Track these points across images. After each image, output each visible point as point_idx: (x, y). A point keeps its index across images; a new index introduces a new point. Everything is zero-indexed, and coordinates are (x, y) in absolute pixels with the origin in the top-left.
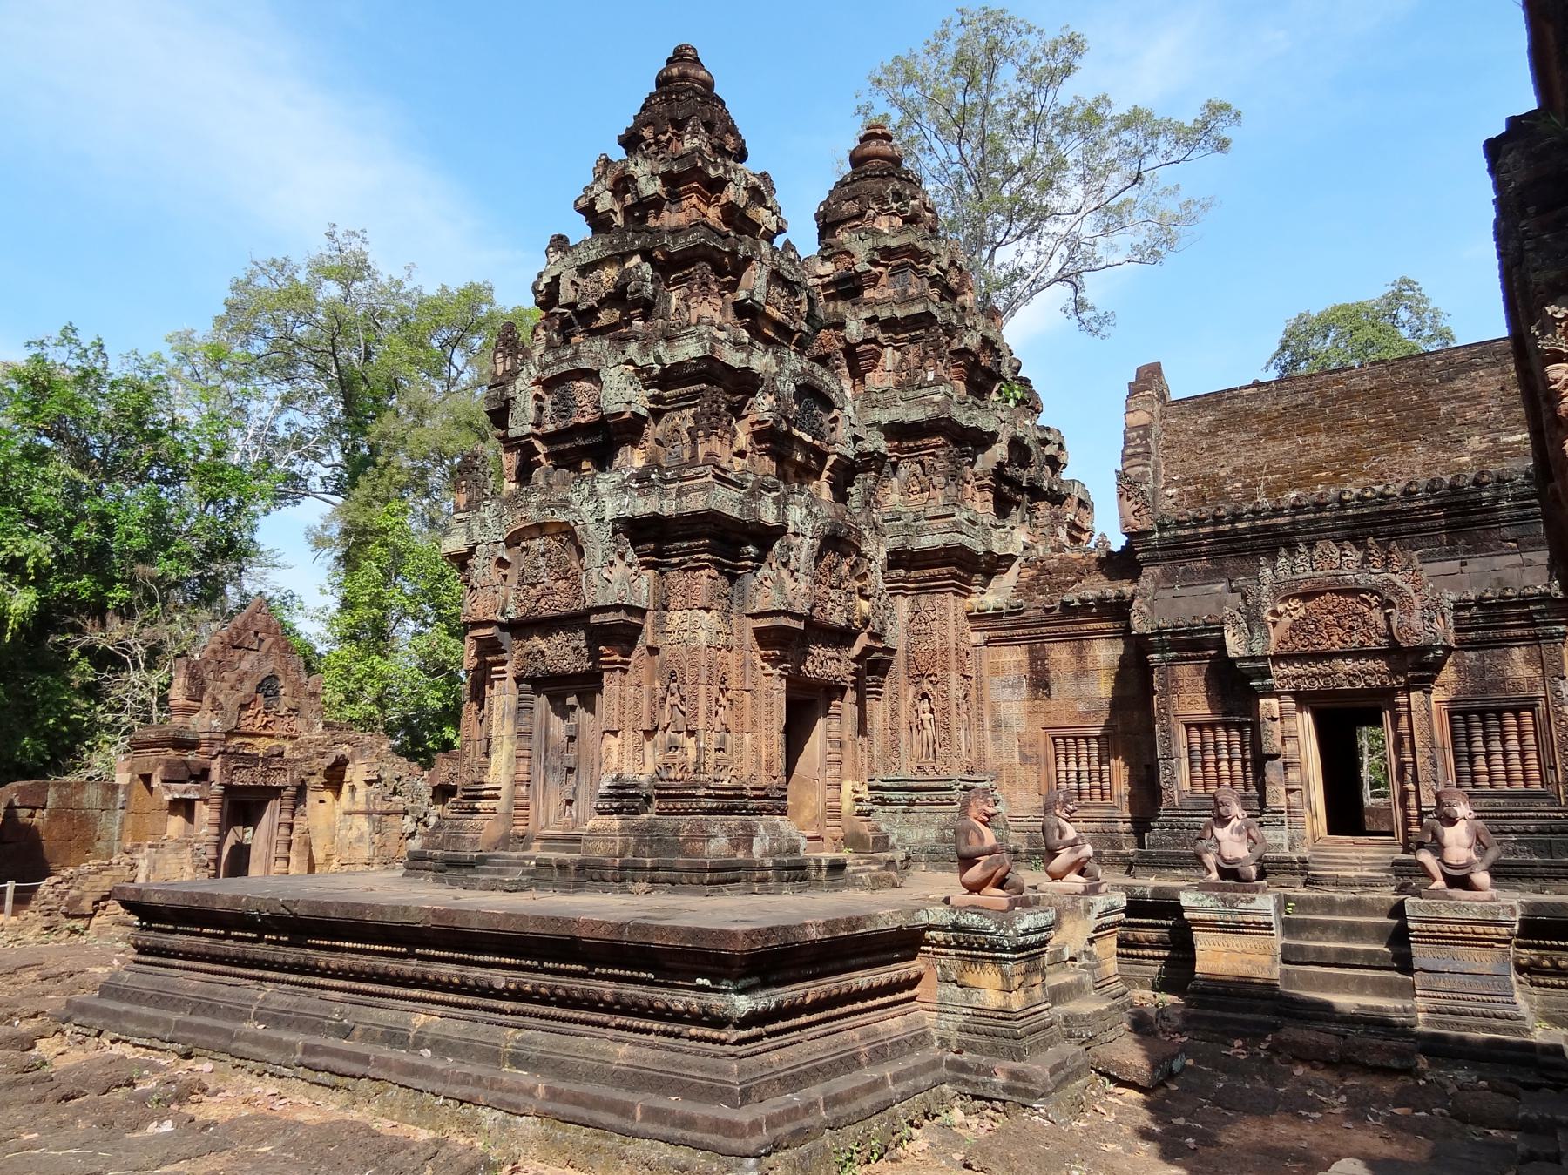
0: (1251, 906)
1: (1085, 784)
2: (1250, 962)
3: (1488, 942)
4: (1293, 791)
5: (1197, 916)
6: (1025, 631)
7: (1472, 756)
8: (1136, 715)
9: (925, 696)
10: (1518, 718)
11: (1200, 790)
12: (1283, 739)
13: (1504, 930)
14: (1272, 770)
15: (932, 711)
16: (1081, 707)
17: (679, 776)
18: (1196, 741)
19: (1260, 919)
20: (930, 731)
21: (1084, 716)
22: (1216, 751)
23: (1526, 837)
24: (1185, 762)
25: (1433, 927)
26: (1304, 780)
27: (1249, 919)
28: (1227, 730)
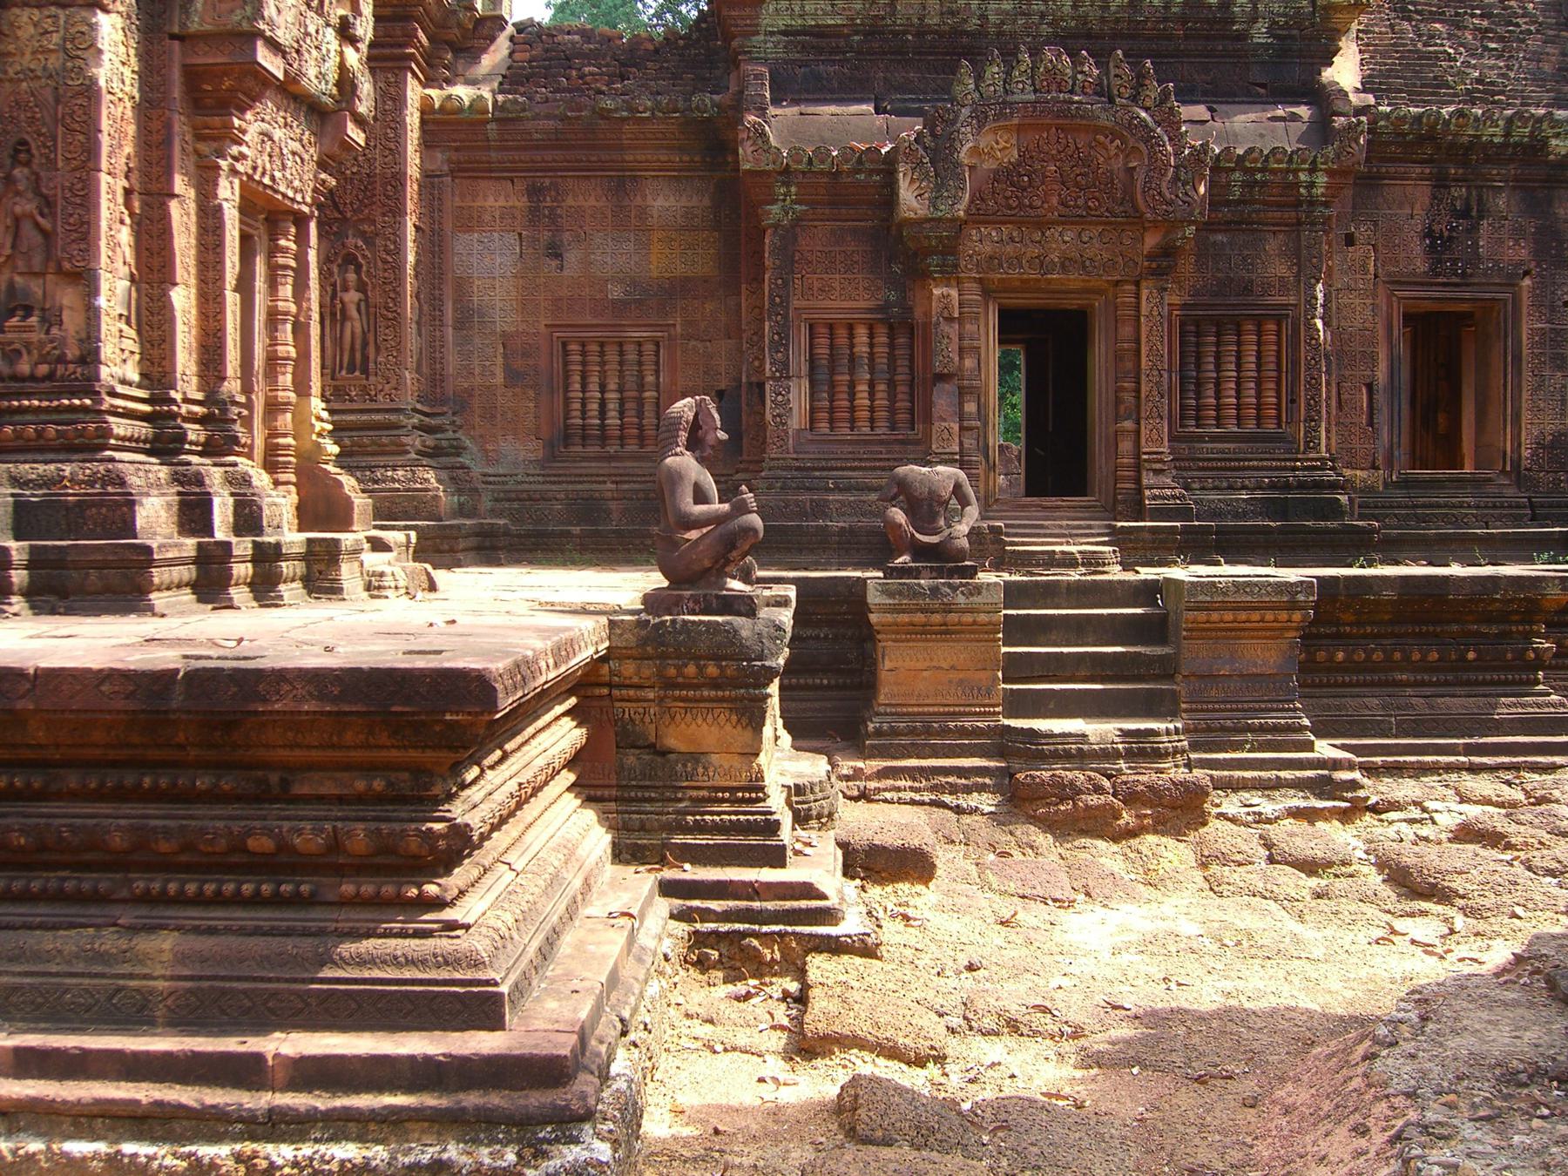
0: (975, 599)
1: (613, 420)
2: (961, 681)
3: (1276, 632)
4: (970, 429)
5: (889, 618)
6: (525, 156)
7: (1199, 384)
8: (709, 307)
9: (350, 260)
10: (1259, 334)
11: (824, 427)
12: (961, 350)
13: (1297, 616)
14: (943, 399)
15: (362, 287)
16: (616, 292)
17: (44, 369)
18: (823, 351)
19: (983, 618)
20: (355, 325)
21: (620, 307)
22: (852, 372)
23: (1259, 495)
24: (805, 383)
25: (1215, 616)
26: (982, 414)
27: (968, 618)
28: (871, 336)
